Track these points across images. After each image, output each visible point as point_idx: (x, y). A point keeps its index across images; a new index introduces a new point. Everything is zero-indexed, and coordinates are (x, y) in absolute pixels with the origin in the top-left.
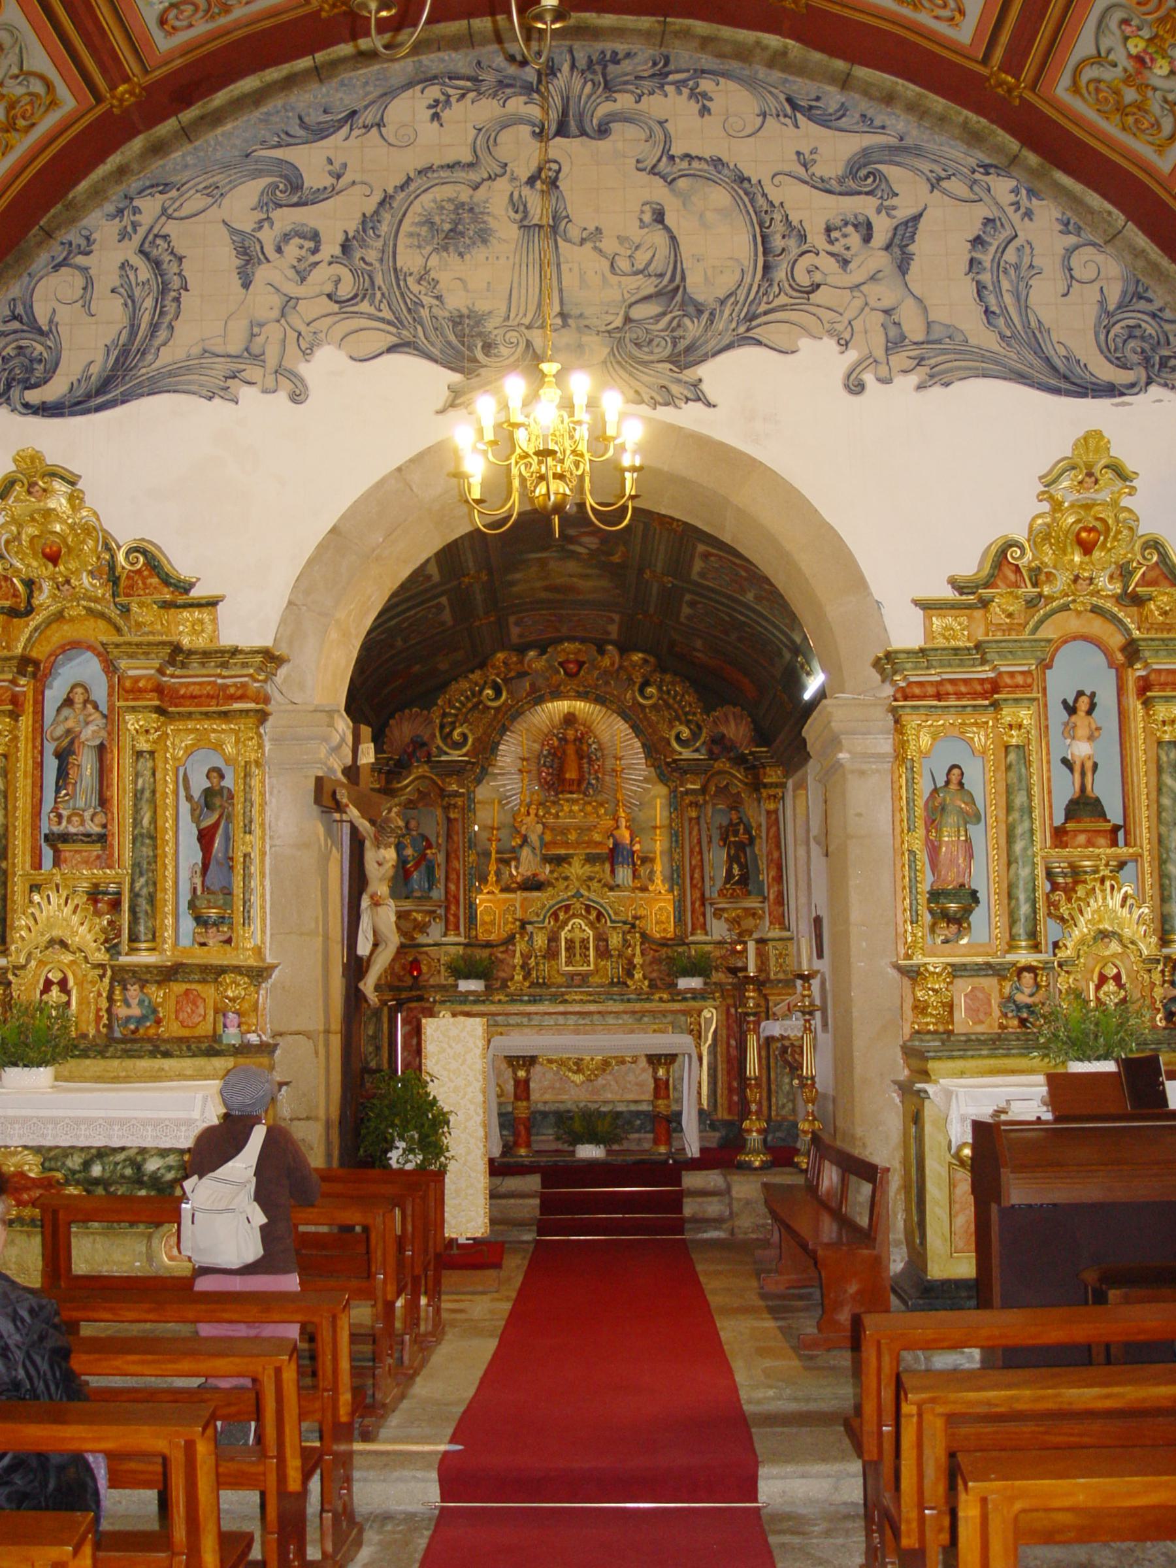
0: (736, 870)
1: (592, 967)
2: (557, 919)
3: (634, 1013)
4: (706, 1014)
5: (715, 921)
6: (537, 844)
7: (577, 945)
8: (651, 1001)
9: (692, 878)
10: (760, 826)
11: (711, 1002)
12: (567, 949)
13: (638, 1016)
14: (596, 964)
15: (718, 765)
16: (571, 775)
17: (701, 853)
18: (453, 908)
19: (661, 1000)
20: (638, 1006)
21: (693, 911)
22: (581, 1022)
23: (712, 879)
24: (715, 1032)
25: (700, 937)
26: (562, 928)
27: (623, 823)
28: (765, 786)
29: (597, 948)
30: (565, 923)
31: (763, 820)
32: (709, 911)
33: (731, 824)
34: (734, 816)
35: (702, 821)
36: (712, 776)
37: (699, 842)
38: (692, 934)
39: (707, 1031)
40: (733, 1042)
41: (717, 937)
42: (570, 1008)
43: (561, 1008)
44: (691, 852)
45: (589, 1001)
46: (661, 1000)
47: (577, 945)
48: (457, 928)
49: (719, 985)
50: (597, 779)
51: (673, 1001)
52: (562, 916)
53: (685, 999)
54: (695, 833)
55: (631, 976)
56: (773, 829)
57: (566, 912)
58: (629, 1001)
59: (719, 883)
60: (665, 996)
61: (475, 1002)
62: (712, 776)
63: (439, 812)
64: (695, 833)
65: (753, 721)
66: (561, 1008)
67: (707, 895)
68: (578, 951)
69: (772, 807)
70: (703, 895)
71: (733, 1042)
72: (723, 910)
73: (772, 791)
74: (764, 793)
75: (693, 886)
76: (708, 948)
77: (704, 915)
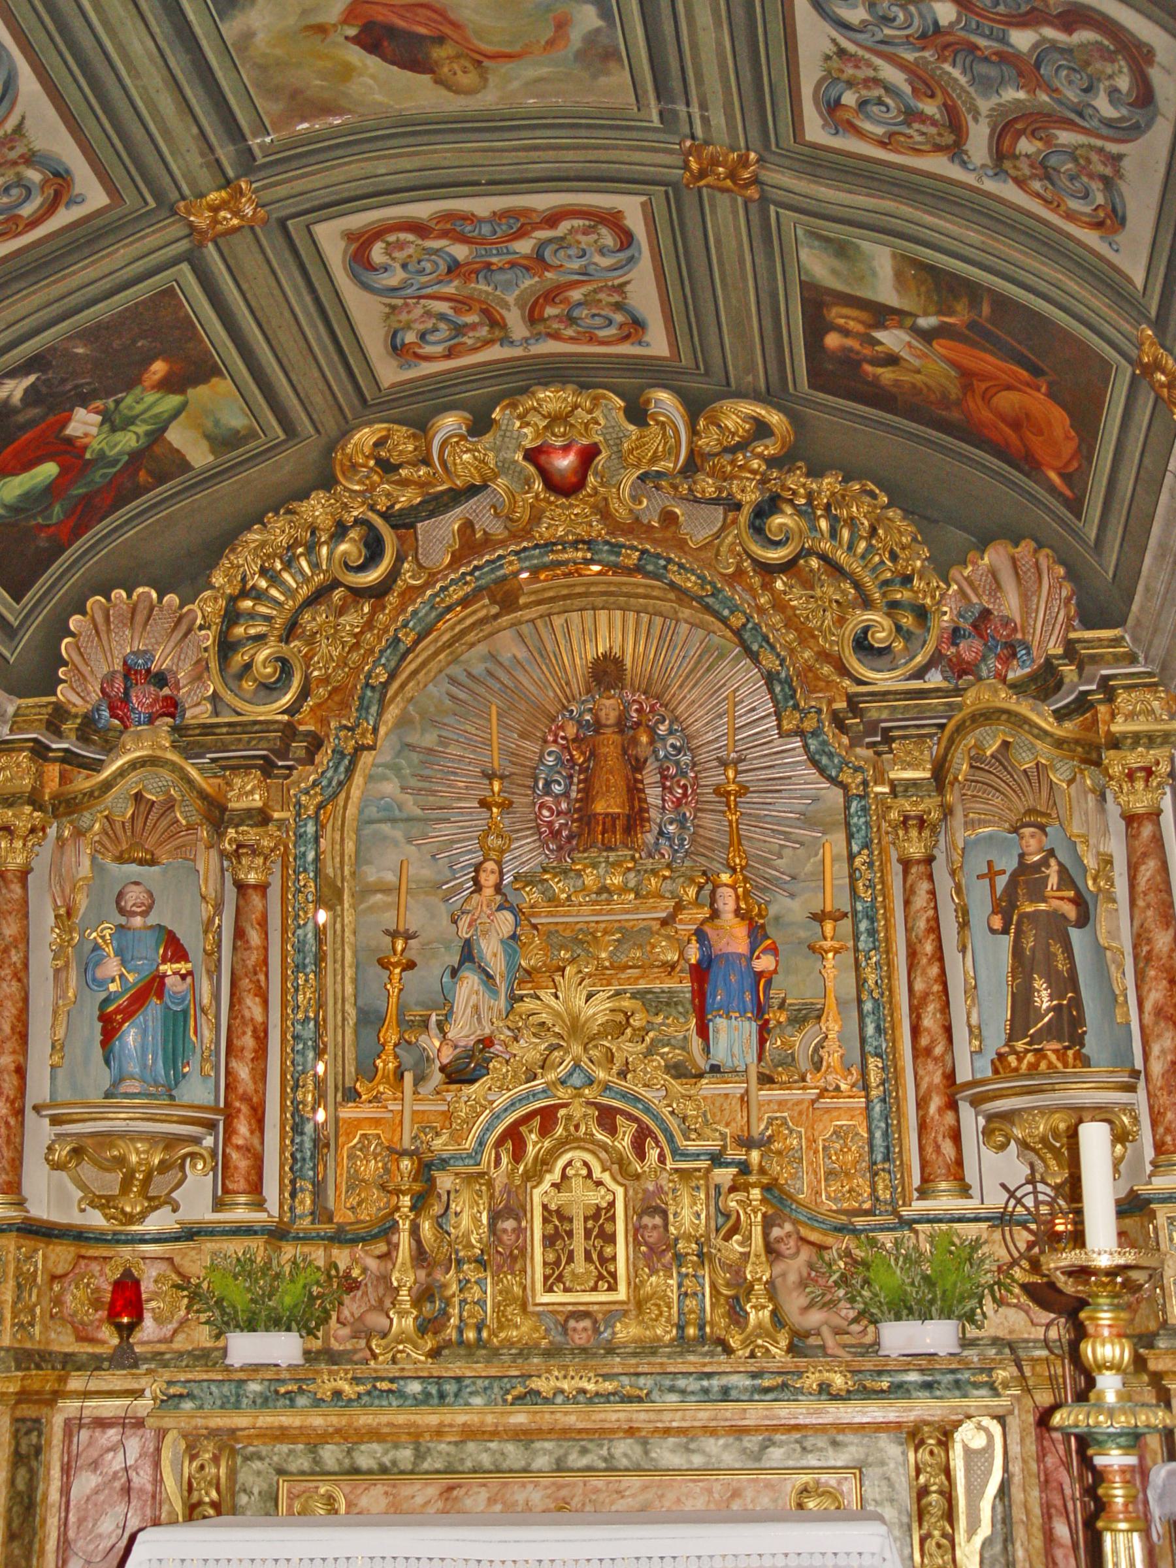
0: (1044, 1000)
1: (622, 1294)
2: (518, 1155)
3: (740, 1431)
4: (968, 1436)
5: (988, 1153)
6: (497, 964)
7: (578, 1227)
8: (797, 1393)
9: (916, 1031)
10: (1108, 861)
11: (979, 1400)
12: (550, 1241)
13: (751, 1442)
14: (635, 1286)
15: (975, 697)
16: (608, 805)
17: (939, 956)
18: (243, 1128)
19: (824, 1389)
20: (755, 1413)
21: (922, 1127)
22: (575, 1460)
23: (975, 1032)
24: (1004, 1491)
25: (945, 1202)
26: (535, 1175)
27: (727, 902)
28: (1115, 743)
29: (636, 1233)
30: (544, 1163)
31: (1116, 847)
32: (971, 1121)
33: (1023, 867)
34: (1032, 844)
35: (940, 869)
36: (960, 729)
37: (935, 928)
38: (923, 1194)
39: (974, 1496)
40: (1062, 1530)
41: (996, 1200)
42: (547, 1417)
43: (520, 1418)
44: (912, 954)
45: (606, 1397)
46: (824, 1389)
47: (578, 1227)
48: (256, 1187)
49: (1010, 1346)
50: (682, 823)
51: (867, 1393)
52: (534, 1145)
53: (899, 1390)
54: (920, 900)
55: (737, 1316)
56: (1148, 869)
57: (544, 1132)
58: (725, 1394)
59: (996, 1040)
60: (838, 1381)
61: (265, 1401)
62: (960, 729)
63: (207, 862)
64: (920, 900)
65: (1072, 575)
66: (520, 1418)
67: (963, 1076)
68: (578, 1244)
69: (1140, 803)
70: (950, 1077)
71: (1062, 1530)
72: (1008, 1117)
73: (1135, 758)
74: (1115, 762)
75: (921, 1053)
76: (970, 1231)
77: (956, 1136)
